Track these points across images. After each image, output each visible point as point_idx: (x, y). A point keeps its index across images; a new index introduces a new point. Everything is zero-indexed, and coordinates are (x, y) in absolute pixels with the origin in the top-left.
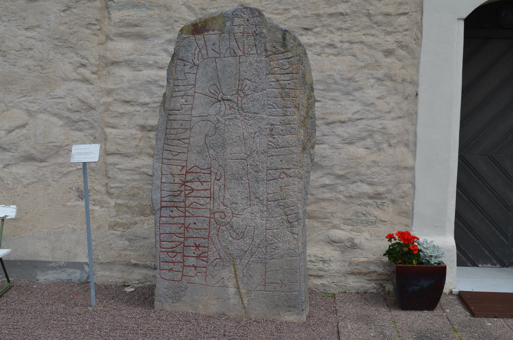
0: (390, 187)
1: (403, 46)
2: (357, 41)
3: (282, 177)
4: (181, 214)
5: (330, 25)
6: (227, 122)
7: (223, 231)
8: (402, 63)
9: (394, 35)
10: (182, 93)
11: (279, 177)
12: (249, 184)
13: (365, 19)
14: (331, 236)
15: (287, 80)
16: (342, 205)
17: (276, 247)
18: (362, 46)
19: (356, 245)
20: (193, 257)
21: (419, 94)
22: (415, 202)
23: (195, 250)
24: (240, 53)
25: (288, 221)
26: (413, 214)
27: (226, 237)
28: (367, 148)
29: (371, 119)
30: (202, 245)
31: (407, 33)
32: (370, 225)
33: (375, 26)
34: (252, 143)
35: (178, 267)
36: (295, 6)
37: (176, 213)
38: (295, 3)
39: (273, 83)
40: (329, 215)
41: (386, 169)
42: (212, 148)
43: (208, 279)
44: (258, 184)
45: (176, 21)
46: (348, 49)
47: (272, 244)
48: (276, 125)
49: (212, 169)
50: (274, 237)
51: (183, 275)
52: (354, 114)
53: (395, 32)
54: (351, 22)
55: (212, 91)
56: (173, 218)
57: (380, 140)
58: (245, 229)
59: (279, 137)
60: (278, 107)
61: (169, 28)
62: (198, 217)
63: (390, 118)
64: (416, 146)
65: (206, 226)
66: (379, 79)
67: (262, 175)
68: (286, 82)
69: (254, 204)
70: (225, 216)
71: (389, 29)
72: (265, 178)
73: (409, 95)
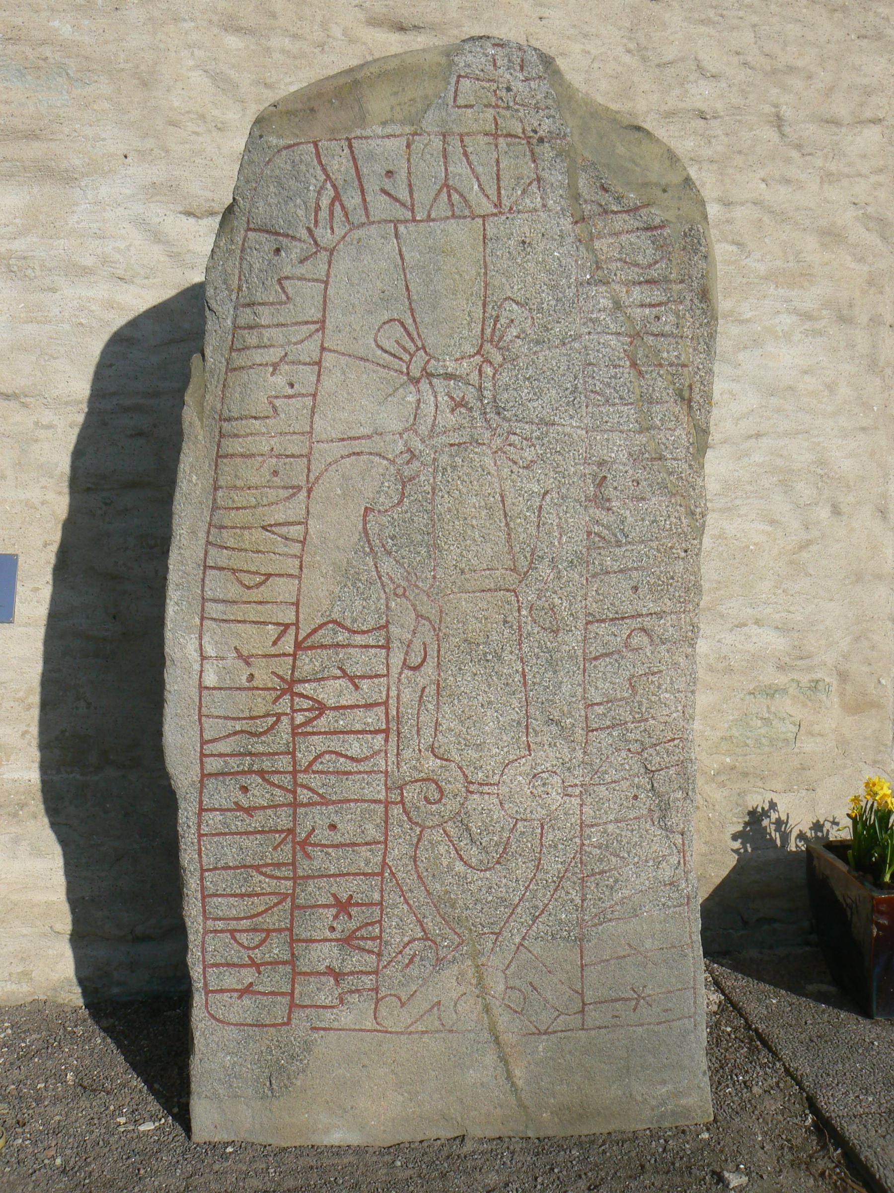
3: (635, 642)
8: (866, 268)
10: (273, 355)
12: (524, 675)
17: (616, 881)
20: (326, 940)
23: (336, 917)
27: (445, 863)
29: (786, 434)
33: (795, 154)
34: (532, 530)
37: (259, 794)
42: (389, 553)
43: (383, 1011)
44: (555, 672)
45: (173, 123)
47: (602, 872)
51: (292, 1006)
56: (249, 811)
58: (511, 831)
60: (621, 398)
61: (150, 143)
66: (807, 316)
67: (572, 641)
68: (647, 311)
71: (832, 167)
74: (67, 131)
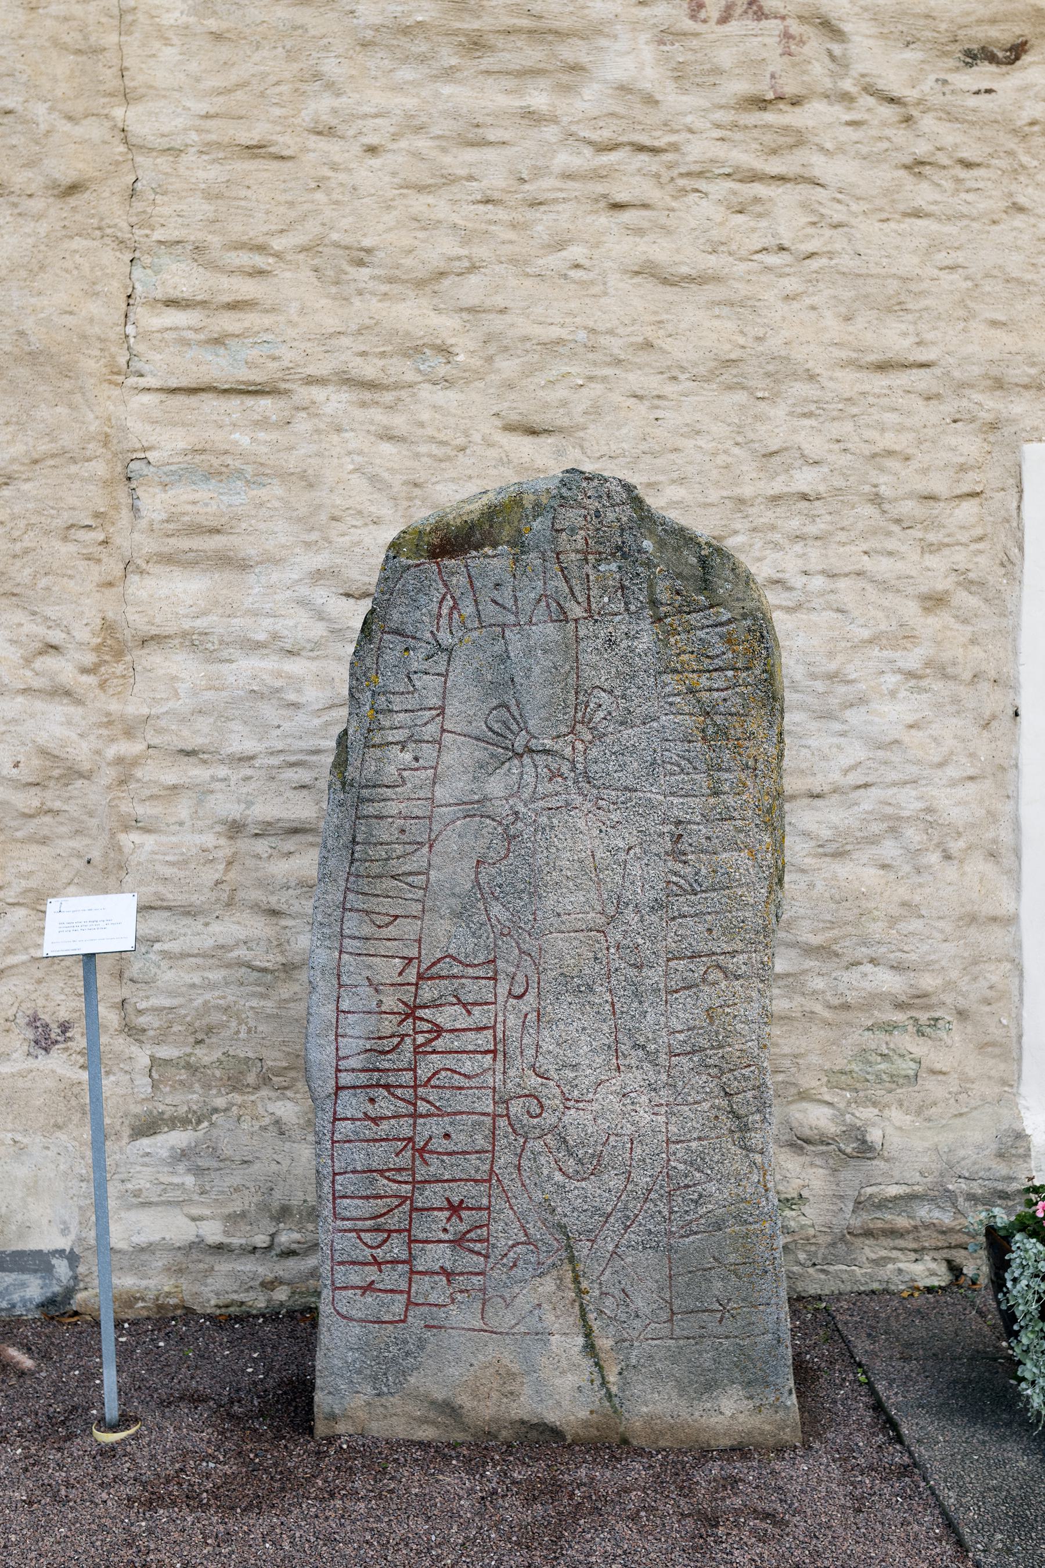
0: (954, 975)
1: (971, 582)
2: (847, 570)
3: (711, 978)
4: (403, 1108)
5: (773, 528)
6: (543, 820)
7: (536, 1155)
8: (970, 628)
9: (946, 551)
11: (704, 980)
12: (613, 1004)
13: (869, 510)
14: (795, 1124)
15: (717, 690)
16: (822, 1032)
17: (701, 1196)
18: (862, 583)
19: (871, 1148)
20: (440, 1241)
21: (1021, 712)
22: (1025, 1014)
23: (449, 1219)
24: (578, 611)
25: (732, 1112)
26: (1021, 1048)
27: (546, 1172)
28: (884, 866)
29: (894, 784)
30: (471, 1203)
31: (980, 546)
32: (902, 1086)
33: (895, 528)
34: (618, 879)
35: (392, 1277)
36: (675, 475)
37: (385, 1105)
38: (675, 467)
39: (678, 699)
40: (787, 1063)
41: (941, 924)
42: (497, 899)
43: (490, 1312)
44: (640, 1003)
45: (334, 519)
46: (822, 594)
47: (687, 1186)
48: (689, 822)
49: (501, 964)
50: (692, 1164)
51: (409, 1303)
52: (846, 772)
53: (948, 545)
54: (829, 518)
55: (496, 727)
56: (376, 1120)
57: (919, 843)
58: (604, 1144)
59: (700, 861)
60: (695, 768)
62: (455, 1114)
63: (944, 782)
64: (1018, 857)
65: (481, 1142)
66: (911, 675)
67: (653, 976)
68: (716, 694)
69: (630, 1067)
70: (542, 1107)
71: (932, 537)
72: (662, 986)
73: (994, 717)
74: (244, 525)
